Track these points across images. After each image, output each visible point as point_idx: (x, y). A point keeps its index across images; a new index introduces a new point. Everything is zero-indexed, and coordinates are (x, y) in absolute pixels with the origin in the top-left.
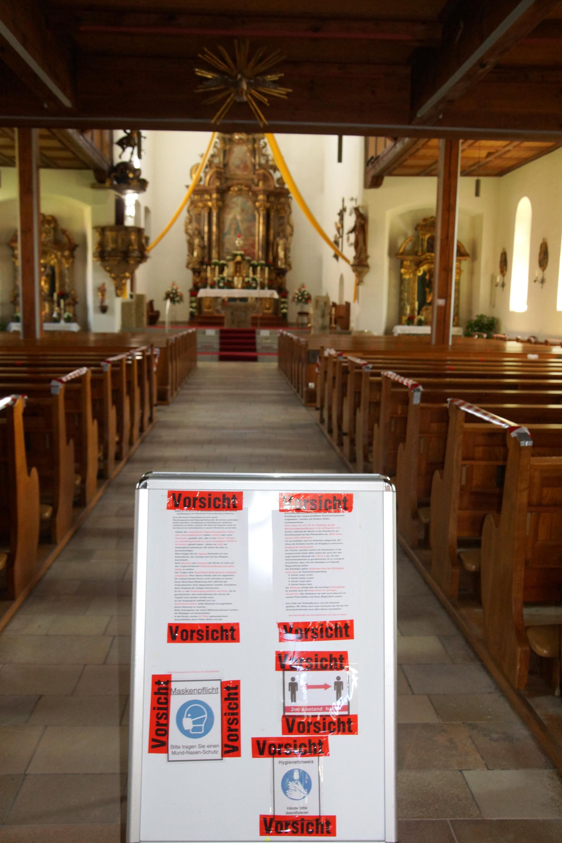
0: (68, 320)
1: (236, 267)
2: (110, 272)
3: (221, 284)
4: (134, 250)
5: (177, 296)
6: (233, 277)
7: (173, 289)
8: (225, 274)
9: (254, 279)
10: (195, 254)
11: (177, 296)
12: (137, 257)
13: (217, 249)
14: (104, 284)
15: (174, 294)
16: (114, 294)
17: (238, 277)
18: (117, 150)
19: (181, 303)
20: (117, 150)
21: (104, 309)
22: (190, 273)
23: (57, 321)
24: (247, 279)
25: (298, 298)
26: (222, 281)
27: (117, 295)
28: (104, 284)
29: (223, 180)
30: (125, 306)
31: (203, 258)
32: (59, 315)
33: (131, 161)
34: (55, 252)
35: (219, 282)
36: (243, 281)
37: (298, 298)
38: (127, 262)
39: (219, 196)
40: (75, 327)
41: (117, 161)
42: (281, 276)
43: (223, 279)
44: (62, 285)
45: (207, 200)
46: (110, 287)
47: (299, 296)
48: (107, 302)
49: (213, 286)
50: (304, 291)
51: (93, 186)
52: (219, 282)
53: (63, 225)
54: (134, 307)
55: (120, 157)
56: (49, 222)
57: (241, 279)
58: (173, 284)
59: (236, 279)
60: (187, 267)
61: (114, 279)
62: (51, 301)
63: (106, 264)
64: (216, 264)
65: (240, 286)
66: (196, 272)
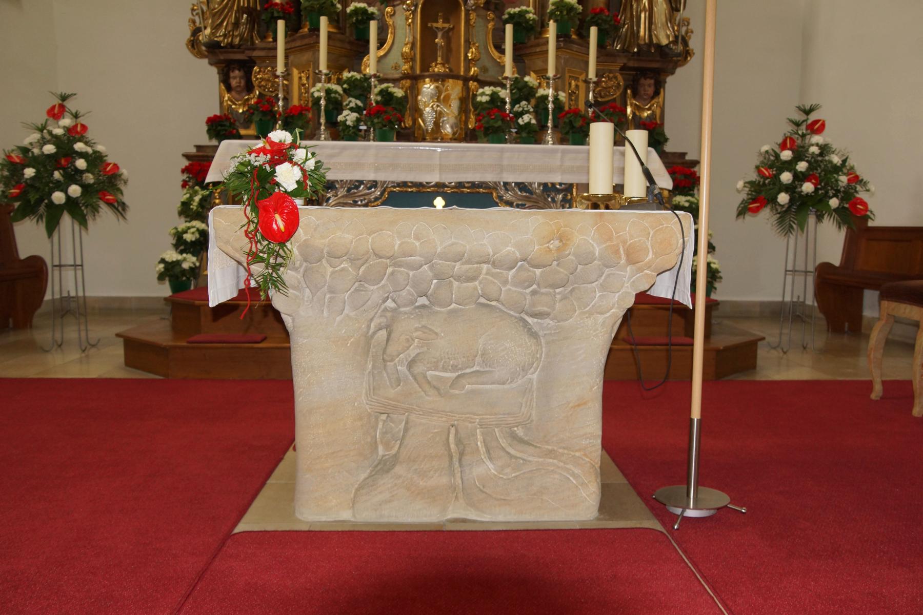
1: (428, 33)
3: (348, 117)
5: (74, 176)
6: (415, 79)
8: (370, 66)
9: (522, 92)
11: (74, 176)
15: (45, 163)
17: (435, 78)
24: (484, 94)
25: (789, 189)
26: (354, 102)
36: (467, 100)
37: (789, 189)
42: (647, 85)
43: (360, 88)
47: (800, 178)
50: (825, 149)
52: (335, 106)
57: (454, 89)
58: (56, 113)
59: (428, 87)
65: (448, 129)
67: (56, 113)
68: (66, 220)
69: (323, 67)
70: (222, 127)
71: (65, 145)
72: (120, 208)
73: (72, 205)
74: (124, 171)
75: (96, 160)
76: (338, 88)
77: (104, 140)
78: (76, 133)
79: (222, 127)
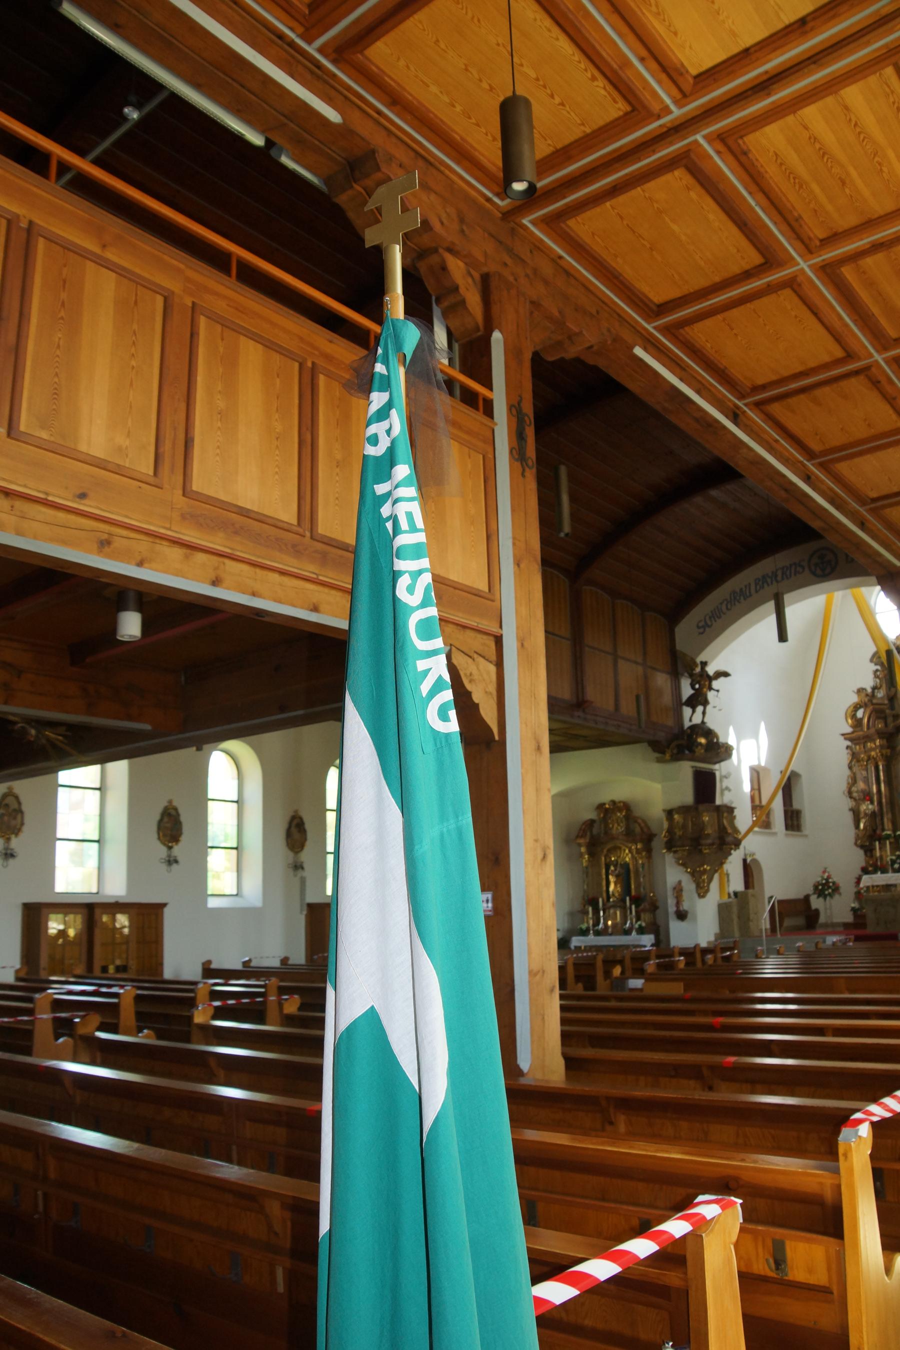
0: (641, 931)
2: (684, 865)
3: (896, 866)
4: (708, 835)
5: (829, 887)
7: (823, 879)
10: (862, 826)
11: (829, 887)
12: (713, 844)
13: (890, 816)
14: (680, 882)
15: (823, 885)
16: (696, 895)
18: (687, 711)
19: (837, 897)
20: (687, 711)
21: (682, 916)
22: (861, 852)
23: (627, 932)
27: (702, 896)
28: (680, 882)
29: (890, 719)
30: (723, 909)
31: (874, 831)
32: (631, 923)
33: (703, 722)
34: (630, 845)
35: (893, 862)
38: (701, 851)
39: (885, 742)
40: (647, 941)
41: (687, 724)
44: (638, 886)
45: (872, 749)
46: (689, 886)
48: (685, 906)
49: (884, 871)
51: (659, 761)
53: (637, 813)
54: (735, 910)
55: (690, 720)
56: (620, 810)
58: (824, 872)
60: (856, 844)
61: (693, 874)
62: (624, 908)
63: (677, 856)
64: (888, 837)
66: (868, 850)
67: (824, 872)
68: (828, 898)
69: (889, 853)
70: (865, 871)
71: (827, 880)
72: (840, 894)
73: (829, 894)
74: (841, 885)
75: (834, 883)
76: (894, 858)
77: (835, 878)
78: (829, 877)
79: (865, 871)
